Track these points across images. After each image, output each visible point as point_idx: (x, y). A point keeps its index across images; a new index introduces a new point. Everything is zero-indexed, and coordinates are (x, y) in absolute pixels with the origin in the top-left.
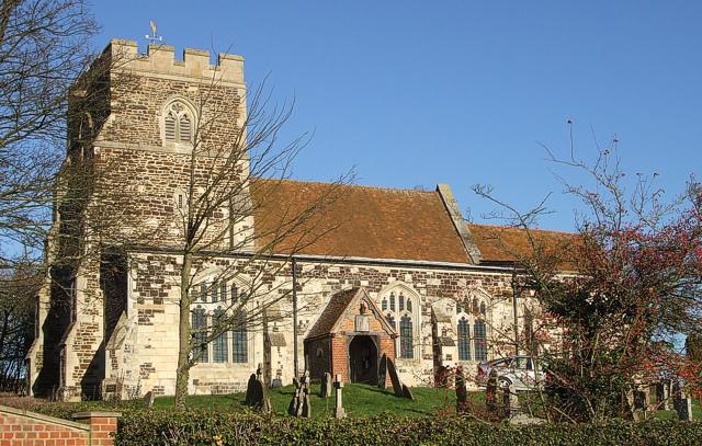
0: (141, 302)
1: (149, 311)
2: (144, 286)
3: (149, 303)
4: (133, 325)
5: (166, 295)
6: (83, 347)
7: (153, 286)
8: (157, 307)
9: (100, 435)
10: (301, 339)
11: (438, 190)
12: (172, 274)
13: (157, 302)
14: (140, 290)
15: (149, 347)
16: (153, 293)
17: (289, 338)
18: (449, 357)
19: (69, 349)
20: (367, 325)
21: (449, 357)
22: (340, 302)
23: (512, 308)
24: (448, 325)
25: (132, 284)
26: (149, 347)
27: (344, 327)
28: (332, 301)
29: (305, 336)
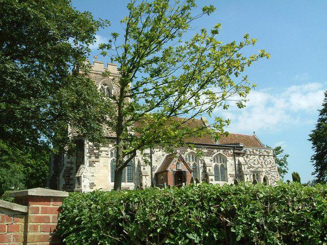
0: (90, 157)
1: (93, 162)
2: (91, 152)
3: (93, 158)
4: (87, 167)
5: (100, 155)
6: (67, 177)
7: (95, 151)
8: (96, 160)
9: (40, 220)
10: (154, 173)
11: (201, 119)
12: (72, 86)
13: (97, 157)
14: (89, 153)
15: (93, 176)
16: (95, 154)
17: (149, 173)
18: (212, 180)
19: (61, 177)
20: (182, 167)
21: (212, 180)
22: (168, 160)
23: (233, 161)
24: (210, 168)
25: (86, 151)
26: (93, 176)
27: (172, 168)
28: (166, 158)
29: (156, 172)
